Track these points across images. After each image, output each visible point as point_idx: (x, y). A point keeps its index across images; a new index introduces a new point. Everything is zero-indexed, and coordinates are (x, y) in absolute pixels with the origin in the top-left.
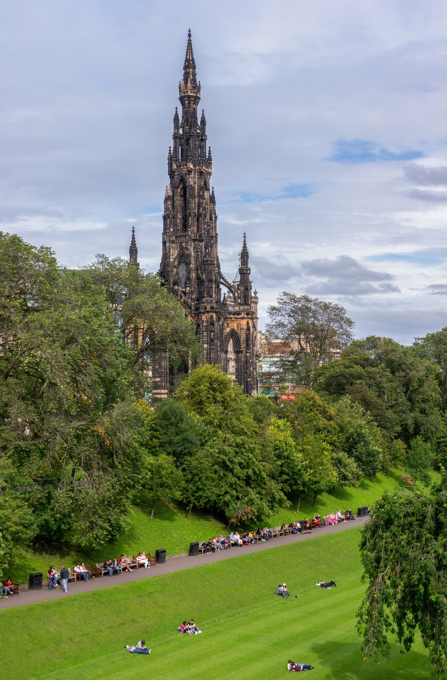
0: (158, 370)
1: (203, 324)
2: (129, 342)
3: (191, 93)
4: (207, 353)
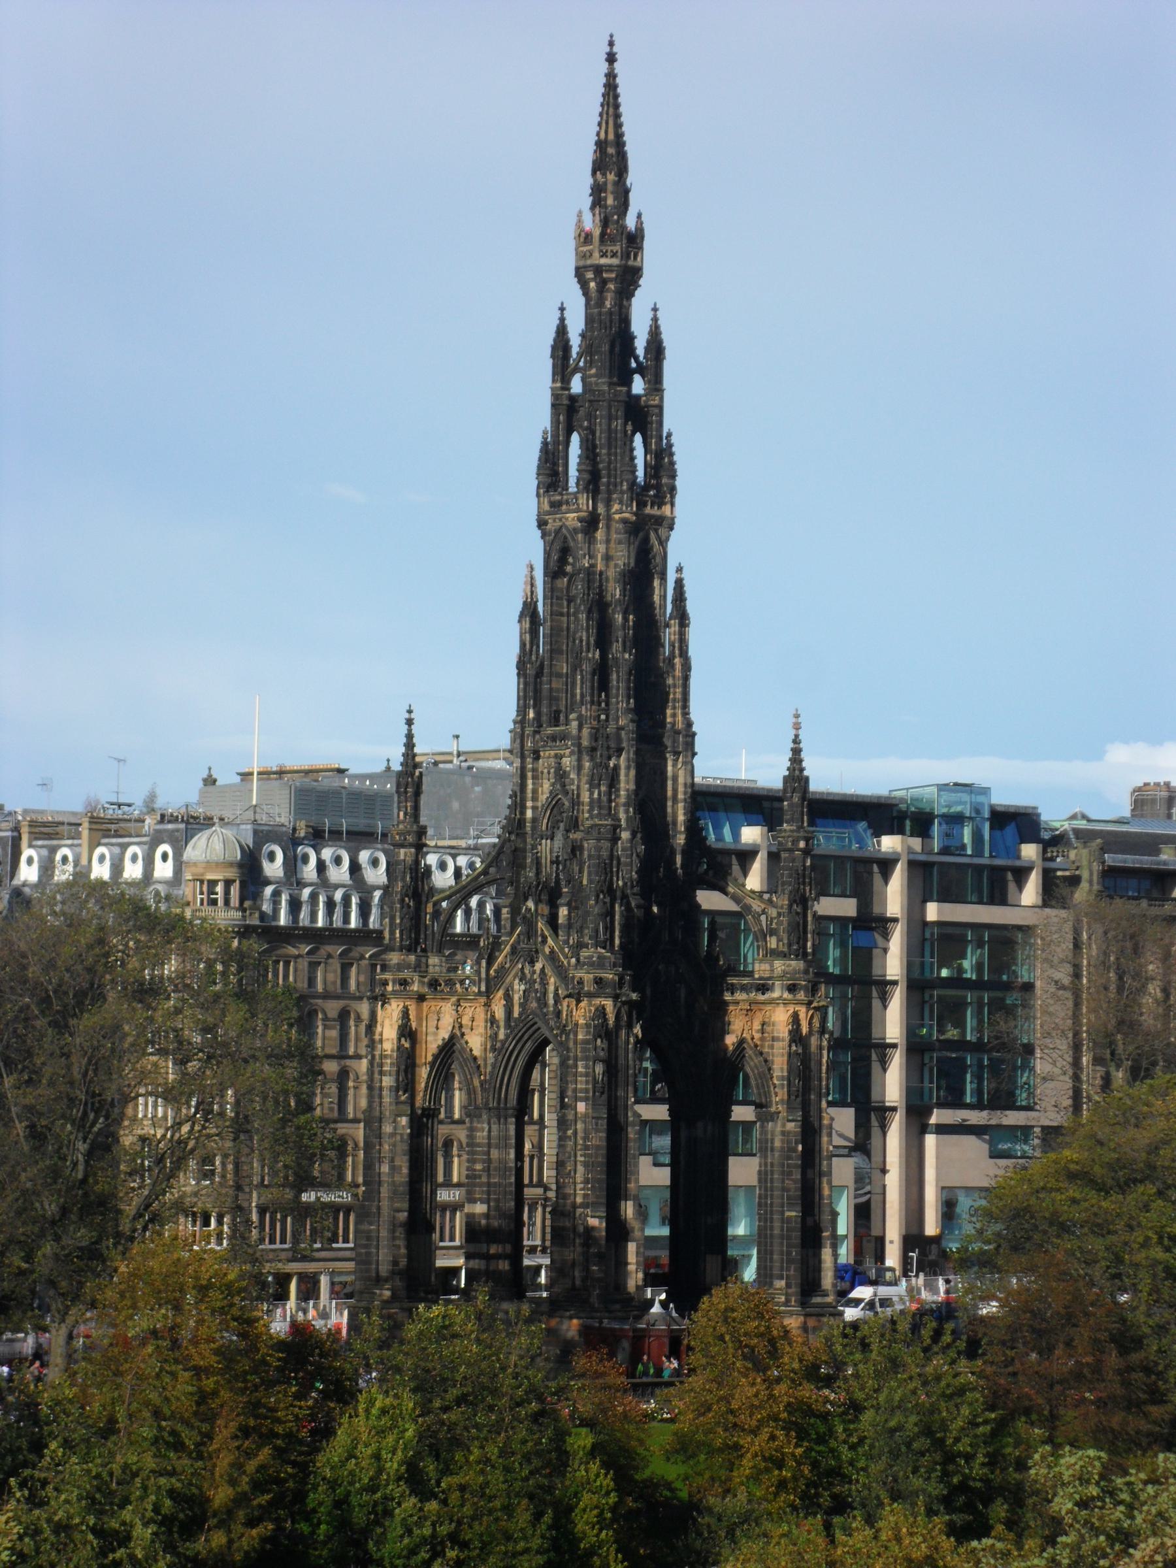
0: (480, 1177)
1: (576, 1035)
2: (384, 1084)
3: (604, 255)
4: (585, 1131)
